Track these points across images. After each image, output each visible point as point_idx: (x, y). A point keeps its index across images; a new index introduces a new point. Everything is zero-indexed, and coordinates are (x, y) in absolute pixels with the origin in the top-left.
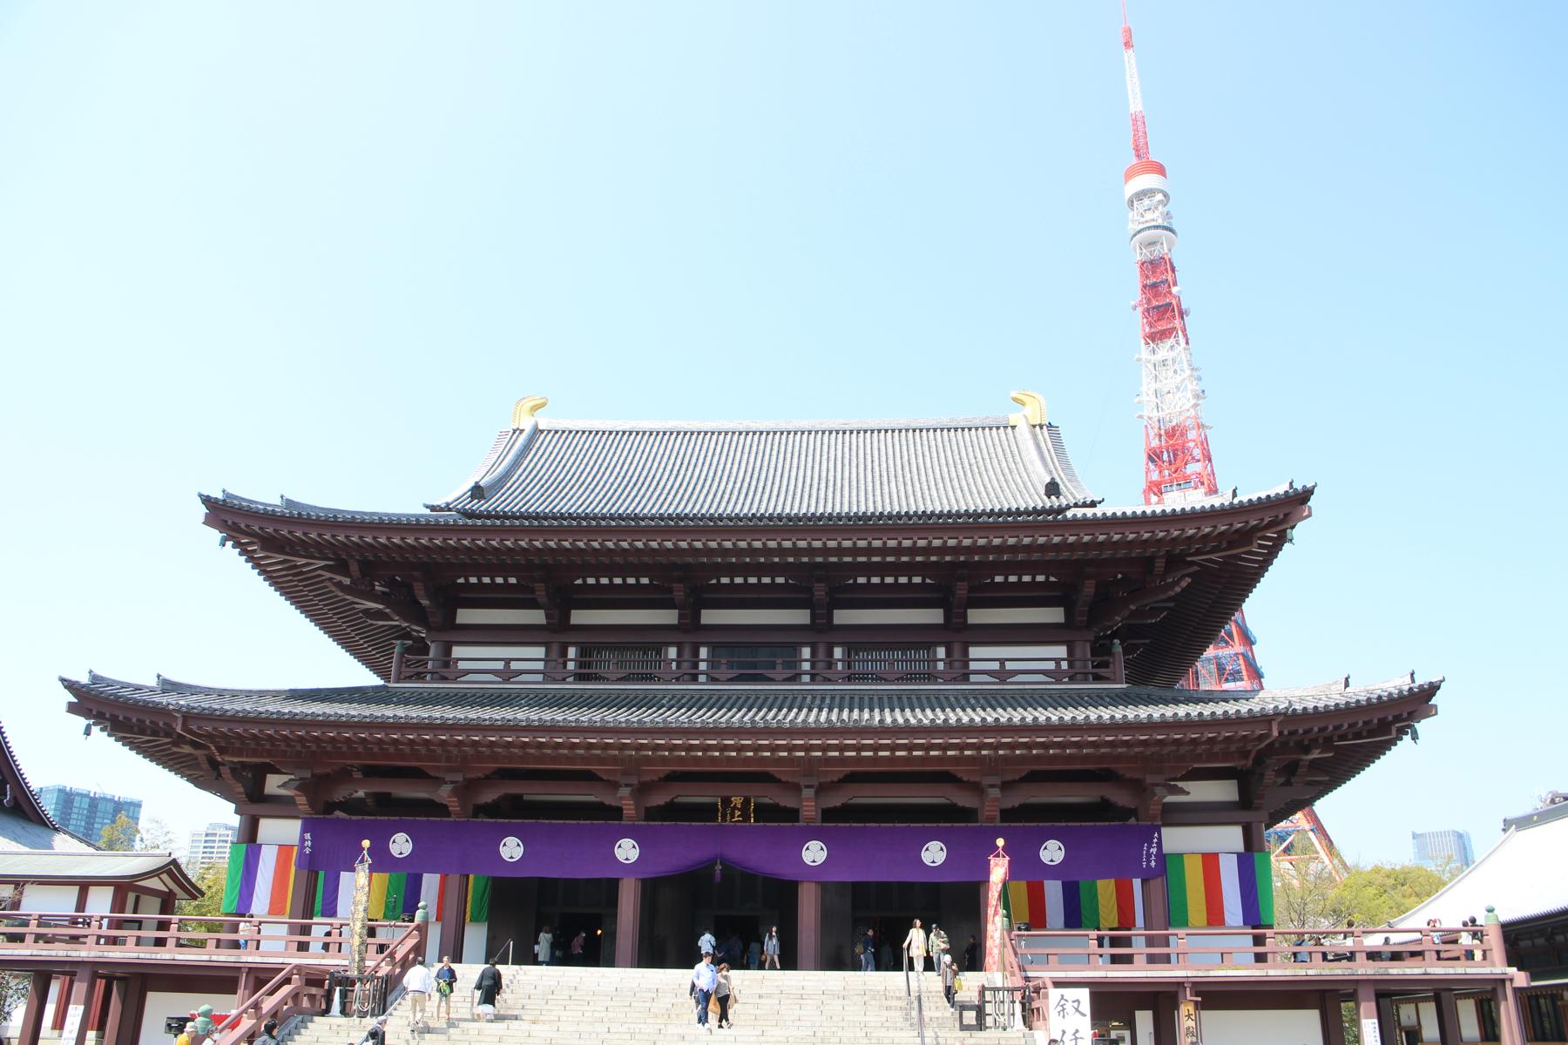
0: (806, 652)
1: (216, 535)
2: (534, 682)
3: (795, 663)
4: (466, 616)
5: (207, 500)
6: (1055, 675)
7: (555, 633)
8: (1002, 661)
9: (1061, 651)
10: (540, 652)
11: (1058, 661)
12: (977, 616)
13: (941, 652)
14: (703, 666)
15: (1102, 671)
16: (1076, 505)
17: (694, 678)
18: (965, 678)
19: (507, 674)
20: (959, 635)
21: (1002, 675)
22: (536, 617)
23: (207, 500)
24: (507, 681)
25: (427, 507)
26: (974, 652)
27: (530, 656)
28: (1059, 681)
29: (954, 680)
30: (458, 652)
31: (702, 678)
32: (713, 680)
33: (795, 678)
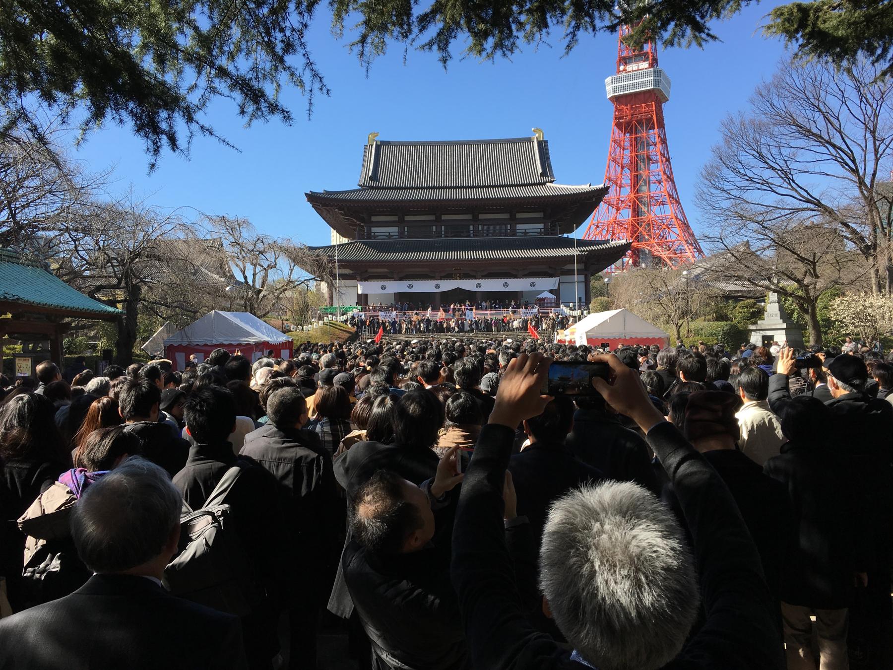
0: (471, 227)
1: (309, 205)
2: (396, 239)
3: (468, 231)
4: (374, 219)
5: (306, 194)
6: (540, 233)
7: (400, 223)
8: (525, 230)
9: (541, 226)
10: (396, 229)
11: (541, 229)
12: (519, 216)
13: (509, 226)
14: (443, 232)
15: (553, 232)
16: (548, 182)
17: (441, 237)
18: (516, 235)
19: (390, 236)
20: (514, 220)
21: (525, 233)
22: (395, 218)
23: (306, 194)
24: (390, 239)
25: (359, 185)
26: (519, 226)
27: (395, 230)
28: (541, 235)
29: (513, 235)
30: (374, 230)
31: (443, 236)
32: (446, 237)
33: (469, 236)
